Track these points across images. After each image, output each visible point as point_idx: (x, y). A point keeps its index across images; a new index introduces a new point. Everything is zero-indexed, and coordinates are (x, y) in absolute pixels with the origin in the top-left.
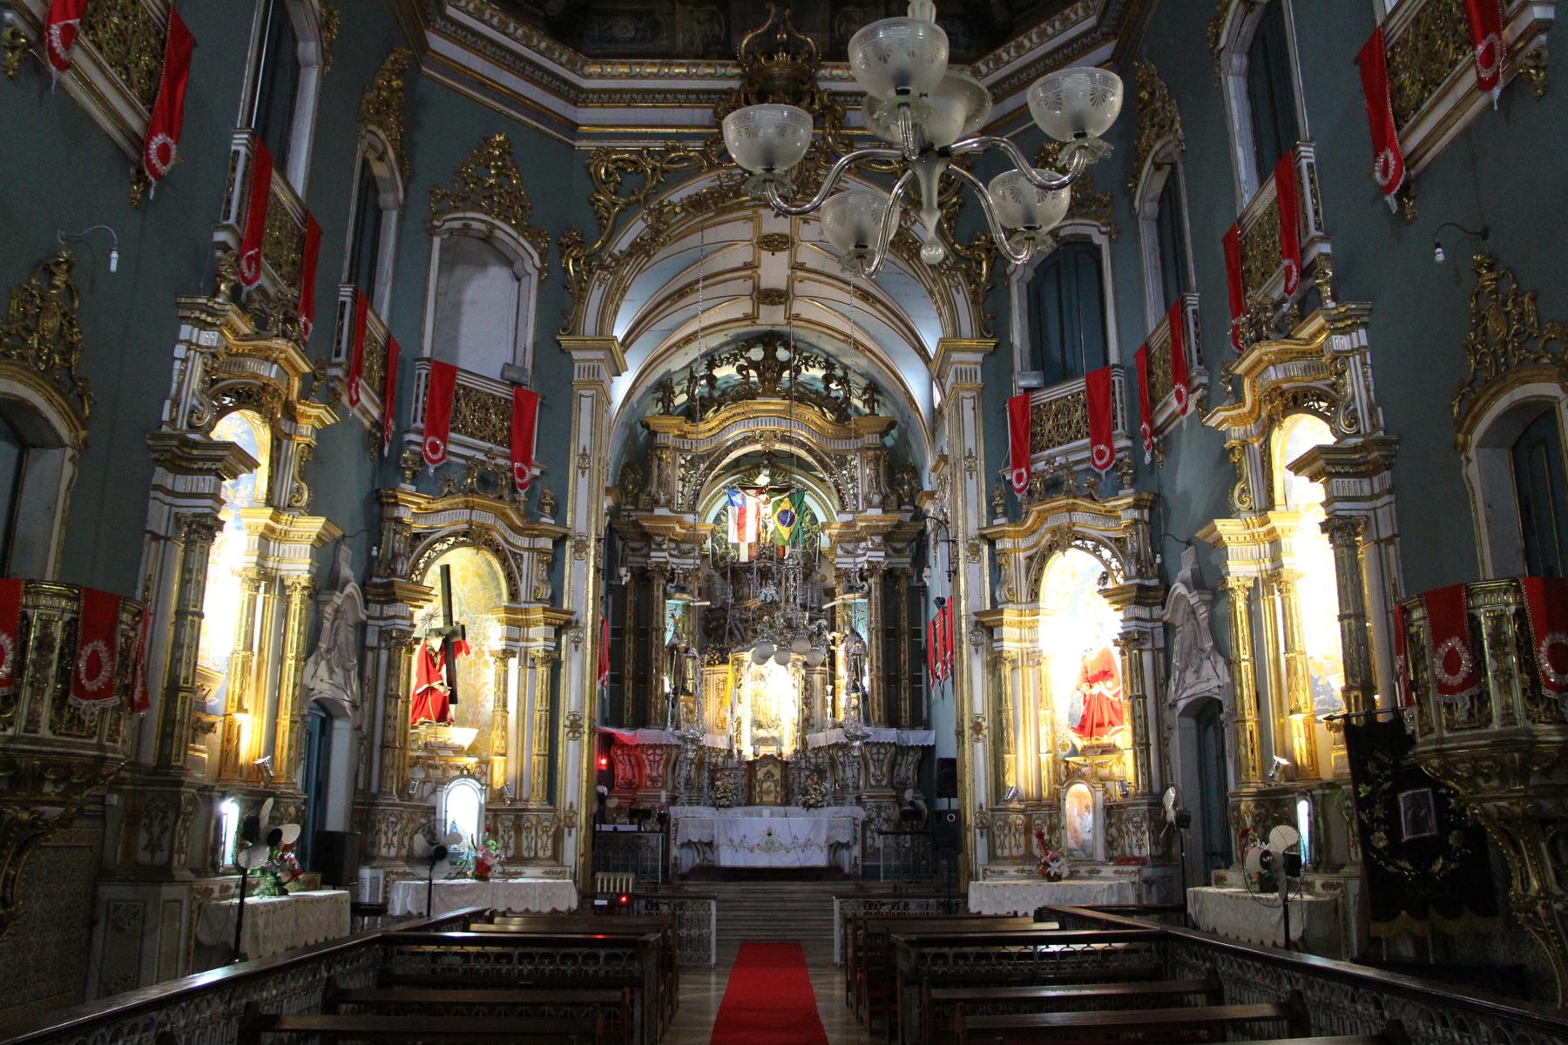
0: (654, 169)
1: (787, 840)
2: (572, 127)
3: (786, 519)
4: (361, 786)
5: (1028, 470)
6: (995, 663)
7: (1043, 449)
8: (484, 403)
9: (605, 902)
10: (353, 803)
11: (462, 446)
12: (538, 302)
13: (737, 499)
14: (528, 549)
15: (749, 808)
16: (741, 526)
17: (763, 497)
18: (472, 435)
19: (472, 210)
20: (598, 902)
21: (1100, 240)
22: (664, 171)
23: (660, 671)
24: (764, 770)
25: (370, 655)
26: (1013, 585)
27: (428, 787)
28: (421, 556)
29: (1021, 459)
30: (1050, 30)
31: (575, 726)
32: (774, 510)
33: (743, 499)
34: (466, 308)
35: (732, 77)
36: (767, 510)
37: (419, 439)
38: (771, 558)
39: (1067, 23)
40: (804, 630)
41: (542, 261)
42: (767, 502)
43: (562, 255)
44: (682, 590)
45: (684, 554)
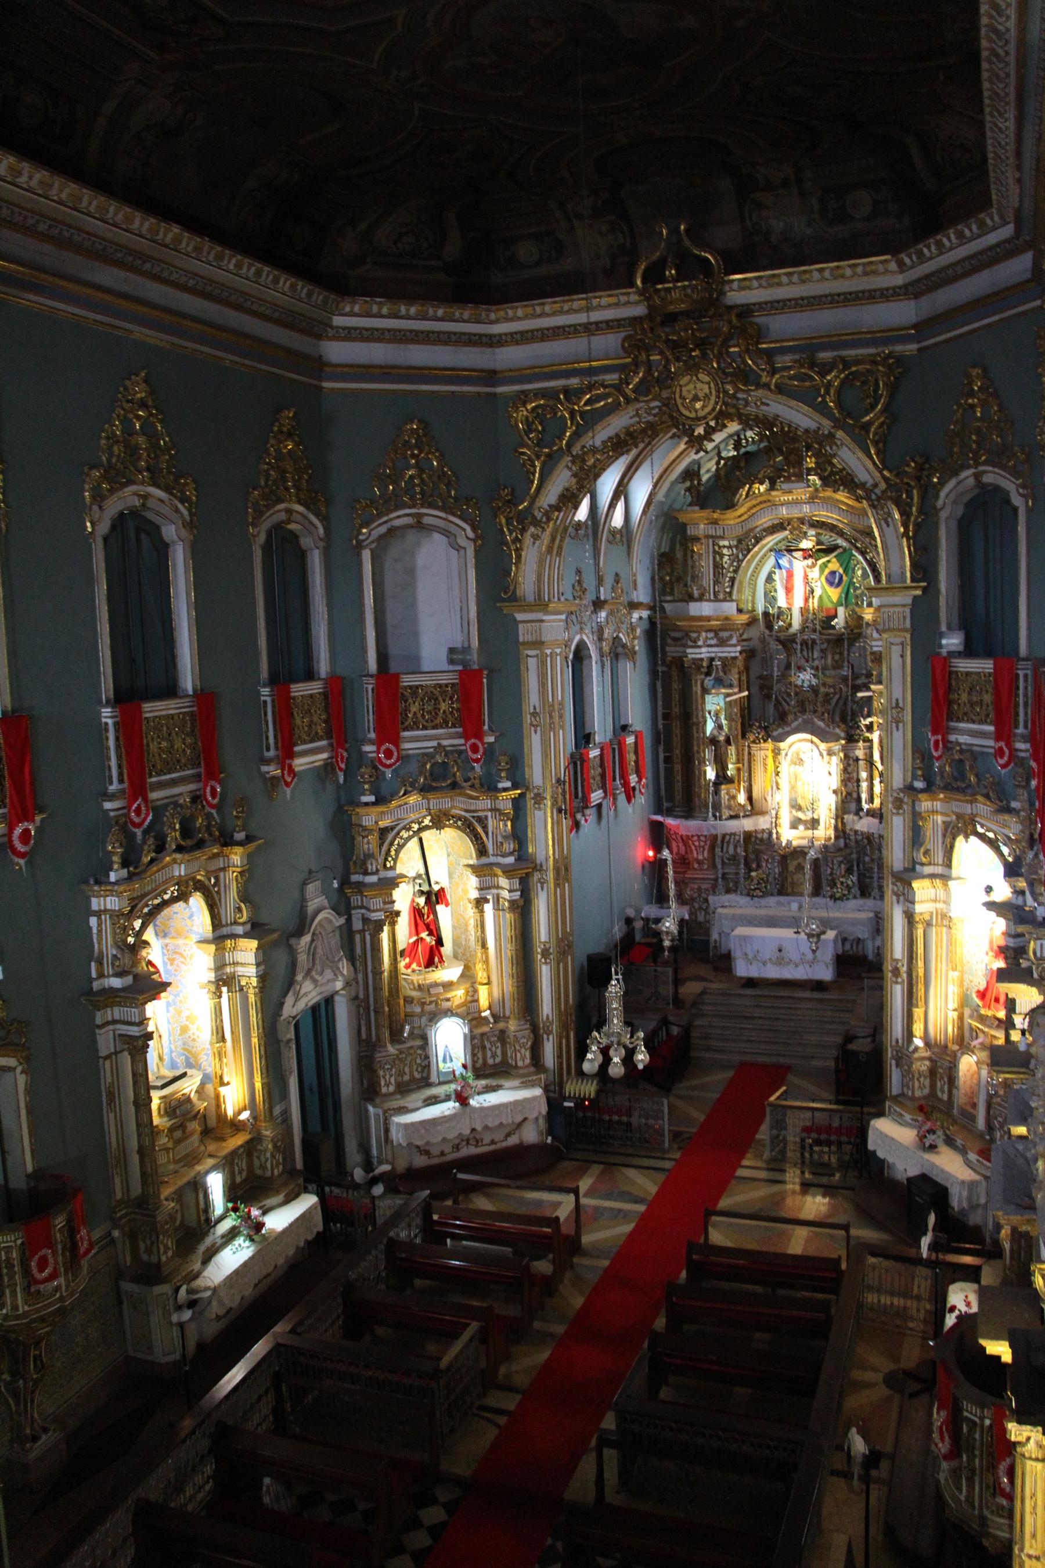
0: (572, 413)
1: (795, 957)
2: (491, 376)
3: (832, 580)
4: (364, 1036)
5: (943, 740)
6: (910, 917)
7: (959, 720)
8: (433, 695)
9: (572, 1104)
10: (359, 1052)
11: (416, 742)
12: (477, 566)
13: (784, 562)
14: (491, 810)
15: (782, 899)
16: (789, 590)
17: (810, 561)
18: (425, 728)
19: (397, 508)
20: (566, 1104)
21: (1017, 501)
22: (582, 414)
23: (702, 762)
24: (795, 863)
25: (358, 937)
26: (930, 847)
27: (424, 1020)
28: (391, 844)
29: (939, 727)
30: (967, 232)
31: (545, 953)
32: (822, 571)
33: (790, 562)
34: (419, 573)
35: (637, 303)
36: (814, 574)
37: (373, 748)
38: (814, 631)
39: (984, 230)
40: (839, 716)
41: (474, 529)
42: (814, 565)
43: (496, 516)
44: (720, 682)
45: (722, 643)
